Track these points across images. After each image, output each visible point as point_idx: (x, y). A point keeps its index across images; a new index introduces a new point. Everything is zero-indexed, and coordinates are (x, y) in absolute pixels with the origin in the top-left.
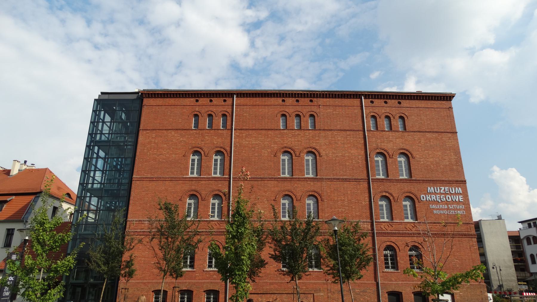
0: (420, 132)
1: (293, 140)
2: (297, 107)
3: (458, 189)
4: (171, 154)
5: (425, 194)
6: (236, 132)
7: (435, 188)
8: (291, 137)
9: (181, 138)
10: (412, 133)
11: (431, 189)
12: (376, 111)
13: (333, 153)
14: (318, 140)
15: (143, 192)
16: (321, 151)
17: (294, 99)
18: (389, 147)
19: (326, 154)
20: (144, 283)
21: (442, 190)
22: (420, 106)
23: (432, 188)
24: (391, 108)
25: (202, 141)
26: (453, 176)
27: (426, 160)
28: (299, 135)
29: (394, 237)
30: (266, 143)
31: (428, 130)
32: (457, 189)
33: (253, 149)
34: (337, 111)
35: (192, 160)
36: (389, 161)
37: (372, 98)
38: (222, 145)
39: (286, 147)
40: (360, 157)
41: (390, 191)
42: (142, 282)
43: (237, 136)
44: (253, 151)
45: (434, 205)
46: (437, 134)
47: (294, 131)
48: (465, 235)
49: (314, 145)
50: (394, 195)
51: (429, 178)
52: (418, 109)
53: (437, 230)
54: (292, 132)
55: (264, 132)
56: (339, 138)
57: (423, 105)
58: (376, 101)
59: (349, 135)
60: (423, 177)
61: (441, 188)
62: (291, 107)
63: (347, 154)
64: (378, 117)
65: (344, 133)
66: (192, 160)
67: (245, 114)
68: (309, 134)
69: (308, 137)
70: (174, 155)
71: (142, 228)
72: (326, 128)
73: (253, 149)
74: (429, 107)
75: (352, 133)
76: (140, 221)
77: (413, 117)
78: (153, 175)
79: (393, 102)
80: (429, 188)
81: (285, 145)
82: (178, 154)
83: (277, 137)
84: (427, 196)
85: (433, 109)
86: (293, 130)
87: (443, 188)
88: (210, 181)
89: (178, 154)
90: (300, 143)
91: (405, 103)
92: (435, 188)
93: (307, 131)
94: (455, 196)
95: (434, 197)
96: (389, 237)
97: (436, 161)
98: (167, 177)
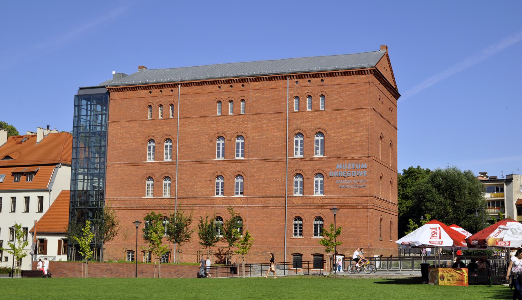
0: (337, 110)
1: (226, 125)
2: (231, 93)
3: (364, 165)
4: (133, 143)
5: (334, 171)
6: (181, 121)
7: (344, 164)
8: (224, 123)
9: (139, 128)
10: (330, 112)
11: (339, 166)
12: (300, 92)
13: (259, 136)
14: (247, 124)
15: (115, 175)
16: (249, 134)
17: (229, 85)
18: (307, 127)
19: (253, 138)
20: (119, 246)
21: (349, 166)
22: (341, 83)
23: (341, 165)
24: (313, 87)
25: (155, 130)
26: (361, 152)
27: (339, 138)
28: (232, 120)
29: (302, 210)
30: (204, 130)
31: (345, 108)
32: (363, 164)
33: (194, 136)
34: (265, 95)
35: (149, 146)
36: (307, 140)
37: (297, 78)
38: (170, 133)
39: (219, 133)
40: (281, 138)
41: (304, 169)
42: (118, 245)
43: (182, 124)
44: (194, 137)
45: (340, 181)
46: (353, 112)
47: (227, 117)
48: (363, 206)
49: (243, 129)
50: (307, 173)
51: (340, 155)
52: (339, 85)
53: (339, 203)
54: (226, 118)
55: (203, 119)
56: (265, 122)
57: (344, 81)
58: (301, 81)
59: (273, 118)
60: (334, 155)
61: (348, 164)
62: (225, 93)
63: (270, 137)
64: (300, 98)
65: (269, 116)
66: (149, 146)
67: (188, 103)
68: (240, 119)
69: (238, 122)
70: (135, 144)
71: (116, 204)
72: (254, 112)
73: (194, 136)
74: (349, 83)
75: (276, 115)
76: (114, 199)
77: (333, 95)
78: (120, 161)
79: (316, 81)
80: (338, 165)
81: (220, 131)
82: (138, 143)
83: (213, 123)
84: (335, 172)
85: (353, 85)
86: (226, 116)
87: (350, 164)
88: (162, 166)
89: (138, 143)
90: (232, 128)
91: (328, 80)
92: (344, 164)
93: (238, 116)
94: (360, 171)
95: (341, 173)
96: (298, 210)
97: (348, 138)
98: (131, 162)
